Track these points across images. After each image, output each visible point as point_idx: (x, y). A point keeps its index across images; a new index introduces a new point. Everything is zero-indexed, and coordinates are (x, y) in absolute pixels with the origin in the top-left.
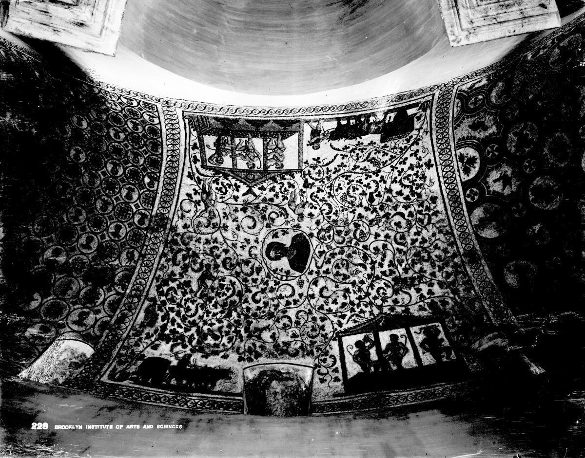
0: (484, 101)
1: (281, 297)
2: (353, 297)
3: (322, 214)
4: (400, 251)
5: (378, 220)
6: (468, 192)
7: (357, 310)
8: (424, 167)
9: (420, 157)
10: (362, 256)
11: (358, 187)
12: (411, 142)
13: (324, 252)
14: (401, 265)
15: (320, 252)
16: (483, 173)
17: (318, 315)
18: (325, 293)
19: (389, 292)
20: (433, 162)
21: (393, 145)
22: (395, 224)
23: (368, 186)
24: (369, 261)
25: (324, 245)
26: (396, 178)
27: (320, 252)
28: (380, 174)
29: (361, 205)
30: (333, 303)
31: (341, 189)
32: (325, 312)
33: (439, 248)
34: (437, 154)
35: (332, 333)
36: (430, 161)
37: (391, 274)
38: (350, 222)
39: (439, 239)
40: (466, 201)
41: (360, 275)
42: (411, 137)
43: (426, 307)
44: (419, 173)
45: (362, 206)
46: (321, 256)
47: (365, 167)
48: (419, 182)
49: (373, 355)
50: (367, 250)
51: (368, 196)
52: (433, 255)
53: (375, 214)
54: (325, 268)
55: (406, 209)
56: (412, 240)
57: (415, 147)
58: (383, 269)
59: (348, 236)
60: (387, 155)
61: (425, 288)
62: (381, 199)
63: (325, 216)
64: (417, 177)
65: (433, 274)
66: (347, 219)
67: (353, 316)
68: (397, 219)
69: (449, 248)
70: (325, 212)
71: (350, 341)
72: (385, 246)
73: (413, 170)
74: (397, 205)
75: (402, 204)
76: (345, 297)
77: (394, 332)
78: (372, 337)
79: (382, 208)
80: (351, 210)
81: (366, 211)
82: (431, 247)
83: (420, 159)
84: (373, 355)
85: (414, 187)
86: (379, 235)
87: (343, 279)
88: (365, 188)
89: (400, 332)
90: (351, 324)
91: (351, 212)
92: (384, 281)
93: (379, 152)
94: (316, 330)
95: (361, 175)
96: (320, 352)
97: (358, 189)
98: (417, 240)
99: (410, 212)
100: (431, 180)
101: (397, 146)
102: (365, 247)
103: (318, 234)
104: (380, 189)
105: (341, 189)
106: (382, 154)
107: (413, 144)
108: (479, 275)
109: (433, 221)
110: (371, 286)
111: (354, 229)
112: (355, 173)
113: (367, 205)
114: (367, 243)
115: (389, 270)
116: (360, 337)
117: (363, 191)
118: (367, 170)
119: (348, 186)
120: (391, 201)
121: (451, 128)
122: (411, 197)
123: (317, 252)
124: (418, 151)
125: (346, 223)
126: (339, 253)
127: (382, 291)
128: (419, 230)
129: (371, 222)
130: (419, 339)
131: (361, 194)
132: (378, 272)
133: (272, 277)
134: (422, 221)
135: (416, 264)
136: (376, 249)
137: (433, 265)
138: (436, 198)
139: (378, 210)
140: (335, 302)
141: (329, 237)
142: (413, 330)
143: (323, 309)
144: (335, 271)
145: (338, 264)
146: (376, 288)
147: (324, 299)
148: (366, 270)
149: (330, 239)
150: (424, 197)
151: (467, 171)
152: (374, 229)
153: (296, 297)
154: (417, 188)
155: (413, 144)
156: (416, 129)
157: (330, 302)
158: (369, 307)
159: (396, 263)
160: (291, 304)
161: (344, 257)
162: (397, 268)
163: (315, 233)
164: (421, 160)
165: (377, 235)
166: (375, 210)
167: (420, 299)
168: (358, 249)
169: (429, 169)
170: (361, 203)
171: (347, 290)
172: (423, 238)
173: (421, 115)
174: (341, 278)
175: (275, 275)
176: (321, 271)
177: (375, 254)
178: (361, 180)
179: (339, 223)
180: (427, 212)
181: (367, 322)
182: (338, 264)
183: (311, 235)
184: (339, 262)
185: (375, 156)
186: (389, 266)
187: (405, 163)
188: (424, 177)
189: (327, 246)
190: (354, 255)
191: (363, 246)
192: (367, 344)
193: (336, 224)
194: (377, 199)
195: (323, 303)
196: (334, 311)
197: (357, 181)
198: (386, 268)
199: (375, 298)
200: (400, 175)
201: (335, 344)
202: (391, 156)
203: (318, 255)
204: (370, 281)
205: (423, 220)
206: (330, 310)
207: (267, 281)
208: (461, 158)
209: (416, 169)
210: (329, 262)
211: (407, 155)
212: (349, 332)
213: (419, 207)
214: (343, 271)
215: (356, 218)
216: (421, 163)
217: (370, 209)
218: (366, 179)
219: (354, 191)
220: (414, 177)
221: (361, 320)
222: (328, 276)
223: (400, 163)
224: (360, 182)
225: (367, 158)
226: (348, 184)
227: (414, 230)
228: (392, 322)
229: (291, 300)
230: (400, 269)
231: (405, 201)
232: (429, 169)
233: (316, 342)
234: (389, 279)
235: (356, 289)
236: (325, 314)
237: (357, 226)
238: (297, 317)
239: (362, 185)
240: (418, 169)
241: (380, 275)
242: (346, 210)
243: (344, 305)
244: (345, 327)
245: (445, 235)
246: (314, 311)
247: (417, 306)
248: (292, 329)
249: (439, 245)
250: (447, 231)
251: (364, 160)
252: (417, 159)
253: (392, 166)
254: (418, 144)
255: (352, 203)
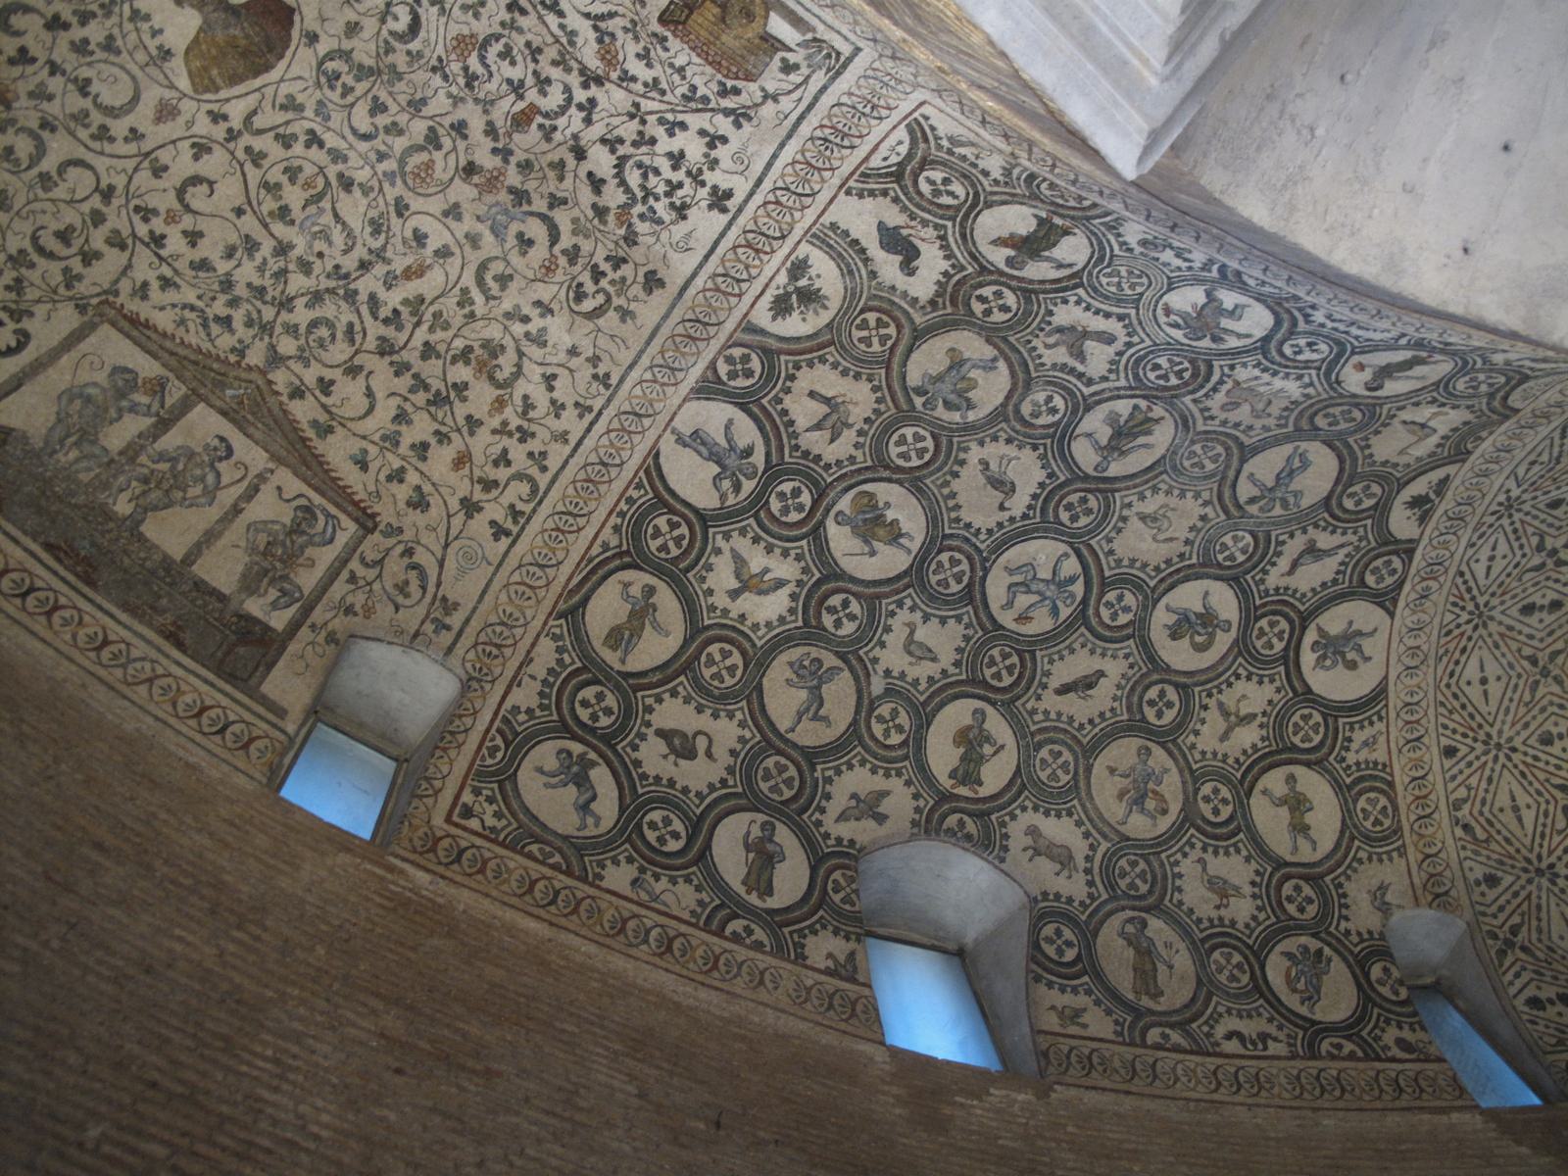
0: (958, 208)
1: (83, 87)
2: (246, 272)
3: (383, 21)
4: (465, 300)
5: (492, 182)
6: (737, 352)
7: (219, 308)
8: (703, 192)
9: (716, 161)
10: (373, 213)
11: (519, 58)
12: (728, 103)
13: (300, 108)
14: (431, 329)
15: (291, 97)
16: (811, 349)
17: (117, 219)
18: (197, 197)
19: (340, 352)
20: (732, 204)
21: (679, 62)
22: (520, 236)
23: (543, 83)
24: (377, 244)
25: (318, 95)
26: (621, 141)
27: (291, 97)
28: (594, 91)
29: (487, 104)
30: (185, 233)
31: (476, 15)
32: (142, 230)
33: (551, 389)
34: (758, 199)
35: (98, 290)
36: (729, 194)
37: (386, 321)
38: (427, 111)
39: (571, 371)
40: (712, 366)
41: (320, 245)
42: (737, 91)
43: (373, 467)
44: (680, 193)
45: (486, 112)
46: (283, 107)
47: (572, 34)
48: (661, 208)
49: (119, 435)
50: (400, 215)
51: (521, 105)
52: (521, 388)
53: (497, 161)
54: (258, 144)
55: (575, 232)
56: (517, 306)
57: (724, 125)
58: (382, 294)
59: (389, 139)
60: (649, 65)
61: (422, 427)
62: (545, 146)
63: (384, 33)
64: (668, 194)
65: (473, 423)
66: (424, 101)
67: (193, 308)
68: (536, 230)
69: (570, 413)
70: (391, 25)
71: (113, 348)
72: (443, 253)
73: (675, 168)
74: (565, 202)
75: (576, 212)
76: (230, 252)
77: (238, 440)
78: (176, 391)
79: (526, 167)
80: (454, 90)
81: (487, 133)
82: (539, 370)
83: (714, 164)
84: (119, 435)
85: (639, 208)
86: (459, 218)
87: (271, 214)
88: (530, 81)
89: (252, 454)
90: (164, 321)
91: (450, 95)
92: (356, 321)
93: (636, 38)
94: (67, 243)
95: (550, 40)
96: (13, 296)
97: (513, 63)
98: (526, 319)
99: (576, 247)
100: (689, 235)
101: (689, 73)
102: (401, 208)
103: (330, 56)
104: (561, 122)
105: (476, 15)
106: (639, 48)
107: (727, 112)
108: (558, 529)
109: (601, 322)
110: (316, 298)
111: (421, 140)
112: (540, 17)
113: (499, 124)
114: (416, 204)
115: (395, 311)
116: (148, 367)
117: (522, 83)
118: (572, 43)
119: (499, 30)
120: (561, 178)
121: (836, 182)
122: (611, 218)
123: (285, 89)
124: (724, 140)
125: (416, 105)
126: (330, 151)
127: (324, 332)
128: (555, 306)
129: (470, 169)
130: (266, 508)
131: (509, 82)
132: (366, 285)
133: (115, 19)
134: (580, 296)
135: (467, 363)
136: (420, 238)
137: (500, 404)
138: (661, 283)
139: (513, 160)
140: (193, 237)
141: (347, 90)
142: (286, 478)
143: (146, 220)
144: (276, 175)
145: (300, 169)
146: (317, 313)
147: (177, 206)
148: (345, 252)
149: (344, 95)
150: (637, 254)
151: (781, 307)
152: (463, 192)
153: (119, 127)
154: (642, 216)
155: (727, 112)
156: (763, 89)
157: (181, 227)
158: (251, 332)
159: (428, 316)
160: (86, 126)
161: (332, 171)
162: (418, 324)
163: (322, 48)
164: (712, 169)
165: (453, 212)
166: (505, 154)
167: (384, 438)
168: (381, 190)
169: (710, 207)
170: (492, 102)
171: (251, 246)
172: (543, 330)
173: (796, 67)
174: (269, 205)
175: (128, 26)
176: (246, 140)
177: (404, 242)
178: (539, 50)
179: (400, 86)
180: (611, 289)
181: (209, 355)
182: (300, 169)
183: (313, 38)
184: (309, 170)
185: (620, 34)
186: (406, 302)
187: (671, 134)
188: (681, 211)
189: (320, 103)
190: (357, 192)
191: (398, 201)
192: (144, 400)
193: (391, 83)
194: (533, 134)
195: (162, 209)
196: (164, 253)
197: (528, 44)
198: (393, 299)
199: (292, 330)
200: (635, 144)
201: (67, 319)
202: (655, 80)
203: (281, 100)
204: (325, 283)
205: (585, 295)
206: (158, 240)
207: (94, 15)
208: (799, 268)
209: (680, 175)
210: (286, 141)
211: (695, 121)
212: (136, 328)
213: (608, 259)
214: (294, 196)
215: (447, 121)
216: (707, 176)
217: (496, 139)
218: (555, 63)
219: (503, 55)
220: (661, 189)
221: (195, 337)
222: (248, 167)
223: (661, 121)
224: (535, 52)
225: (602, 17)
226: (503, 24)
227: (544, 292)
228: (257, 411)
229: (97, 118)
230: (421, 335)
231: (590, 213)
232: (710, 207)
233: (32, 266)
234: (375, 329)
235: (274, 265)
236: (134, 235)
237: (433, 139)
238: (62, 169)
239: (531, 66)
240: (687, 181)
241: (363, 297)
242: (445, 78)
243: (203, 265)
244: (144, 310)
245: (595, 377)
246: (116, 202)
247: (355, 446)
248: (13, 179)
249: (556, 384)
250: (607, 375)
251: (587, 16)
252: (706, 155)
253: (637, 105)
254: (738, 125)
255: (471, 79)
